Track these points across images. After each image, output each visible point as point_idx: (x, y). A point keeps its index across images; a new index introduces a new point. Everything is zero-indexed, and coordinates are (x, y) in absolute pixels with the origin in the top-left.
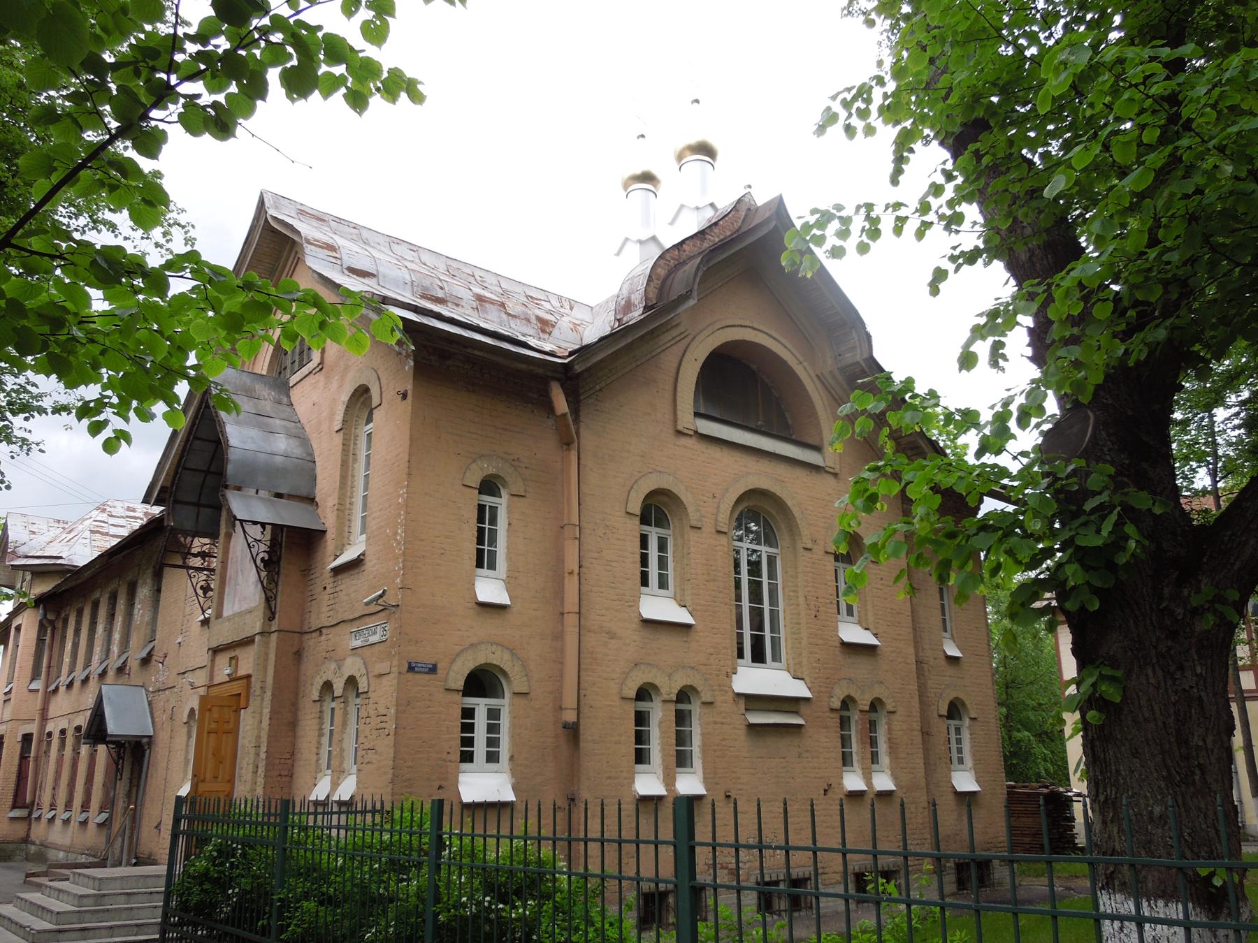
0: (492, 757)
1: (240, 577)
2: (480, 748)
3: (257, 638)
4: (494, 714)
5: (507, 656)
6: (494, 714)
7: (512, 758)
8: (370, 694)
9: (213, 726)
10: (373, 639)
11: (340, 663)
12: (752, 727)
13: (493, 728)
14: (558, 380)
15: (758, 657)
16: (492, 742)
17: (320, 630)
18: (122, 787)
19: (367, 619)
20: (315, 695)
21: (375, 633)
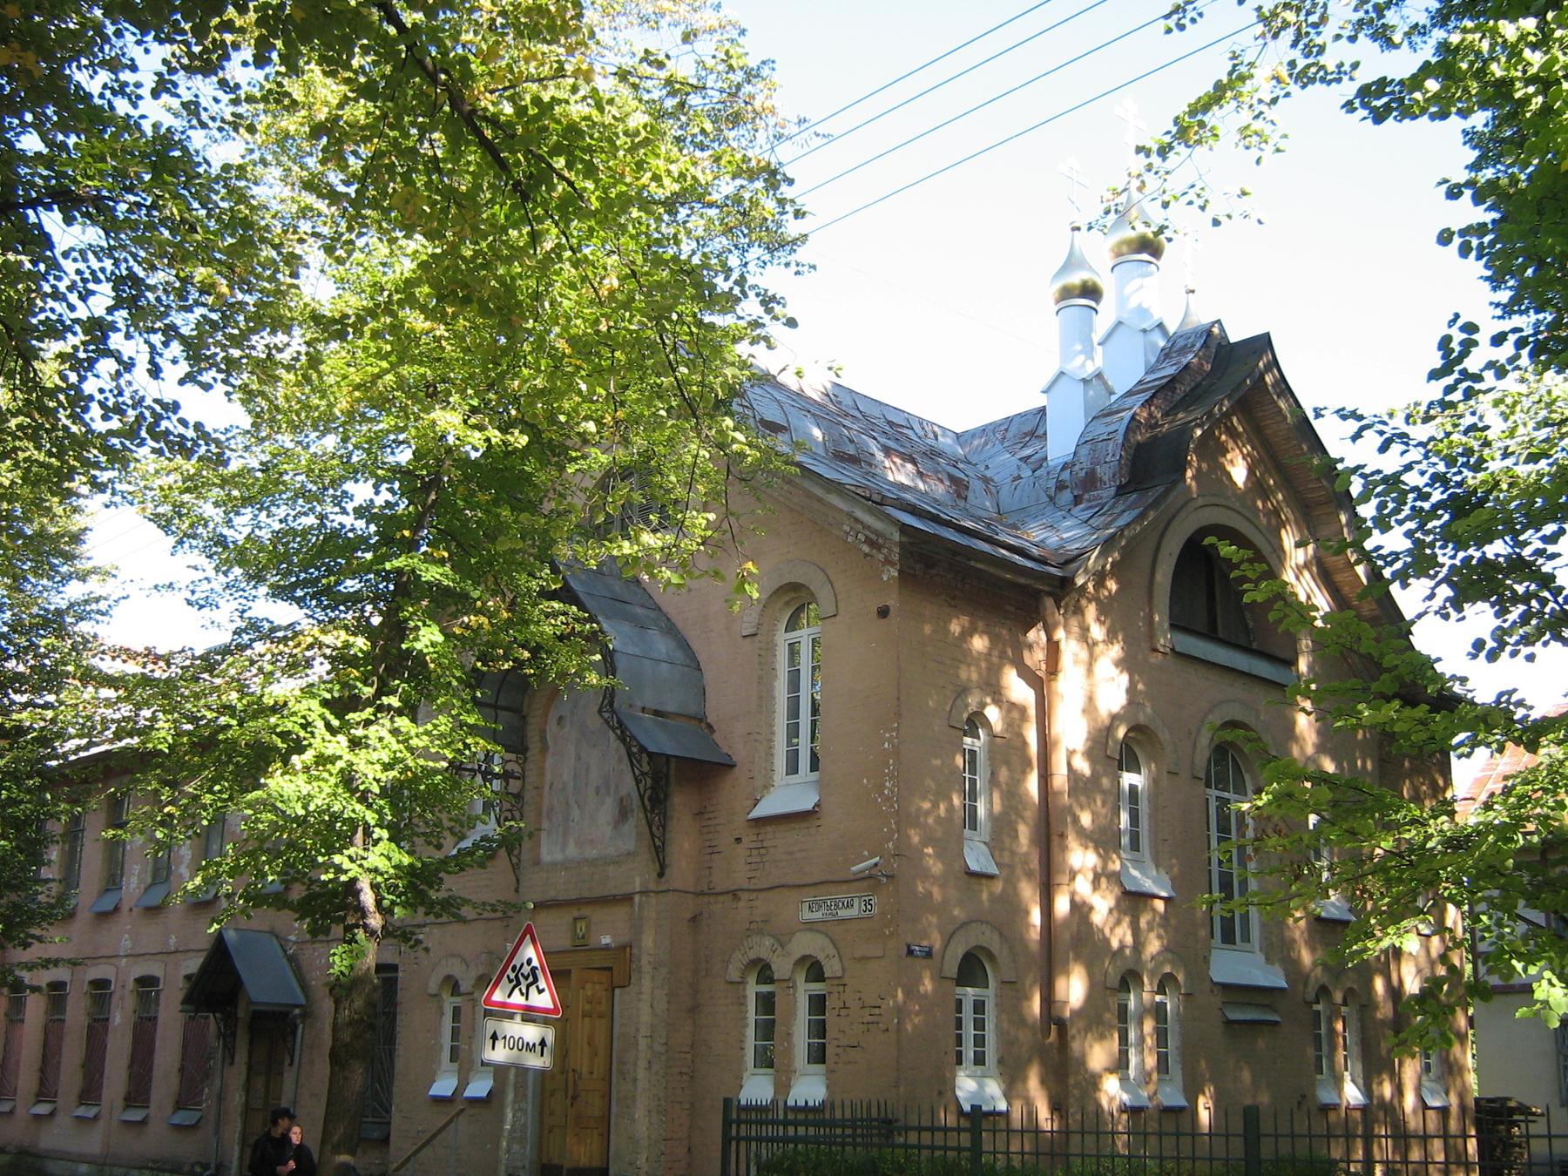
0: (979, 1060)
1: (575, 813)
2: (969, 1052)
3: (637, 898)
4: (979, 1007)
5: (996, 937)
6: (979, 1007)
7: (1001, 1061)
8: (845, 981)
9: (588, 1007)
10: (843, 913)
11: (782, 941)
12: (1229, 1023)
13: (979, 1025)
14: (1049, 594)
15: (1228, 938)
16: (980, 1041)
17: (735, 894)
18: (259, 1083)
19: (833, 888)
20: (734, 974)
21: (849, 906)
